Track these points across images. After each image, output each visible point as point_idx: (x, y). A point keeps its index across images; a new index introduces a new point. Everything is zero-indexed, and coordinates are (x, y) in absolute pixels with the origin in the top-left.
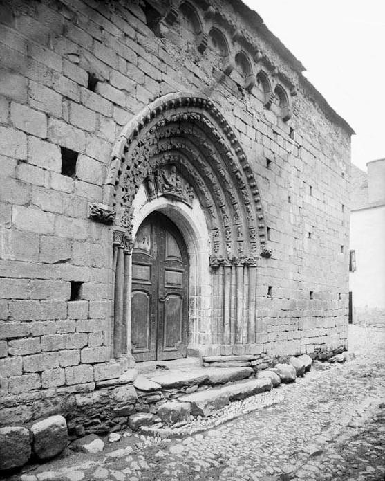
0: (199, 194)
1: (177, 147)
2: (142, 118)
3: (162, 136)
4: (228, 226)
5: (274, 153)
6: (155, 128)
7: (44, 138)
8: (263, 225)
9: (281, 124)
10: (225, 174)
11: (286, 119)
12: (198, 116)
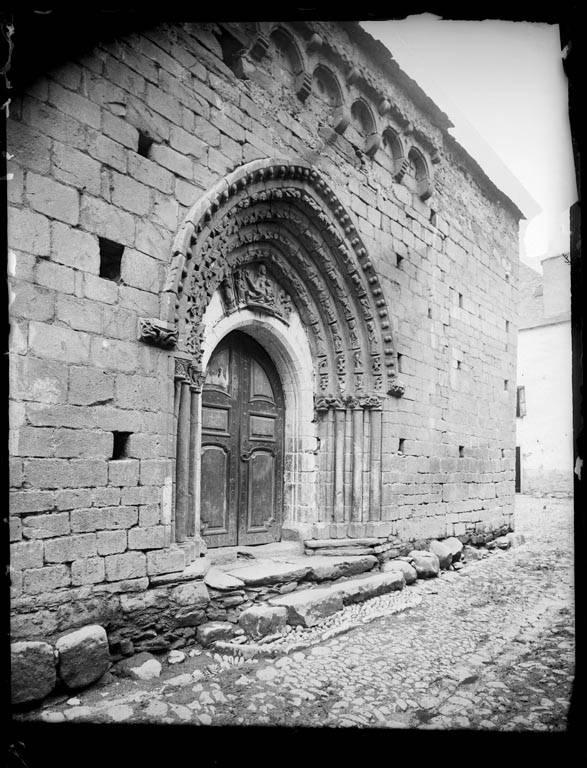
0: (299, 305)
1: (267, 237)
2: (217, 195)
3: (245, 222)
5: (407, 246)
6: (235, 210)
7: (75, 224)
8: (391, 350)
9: (418, 205)
10: (337, 276)
11: (424, 197)
12: (298, 193)
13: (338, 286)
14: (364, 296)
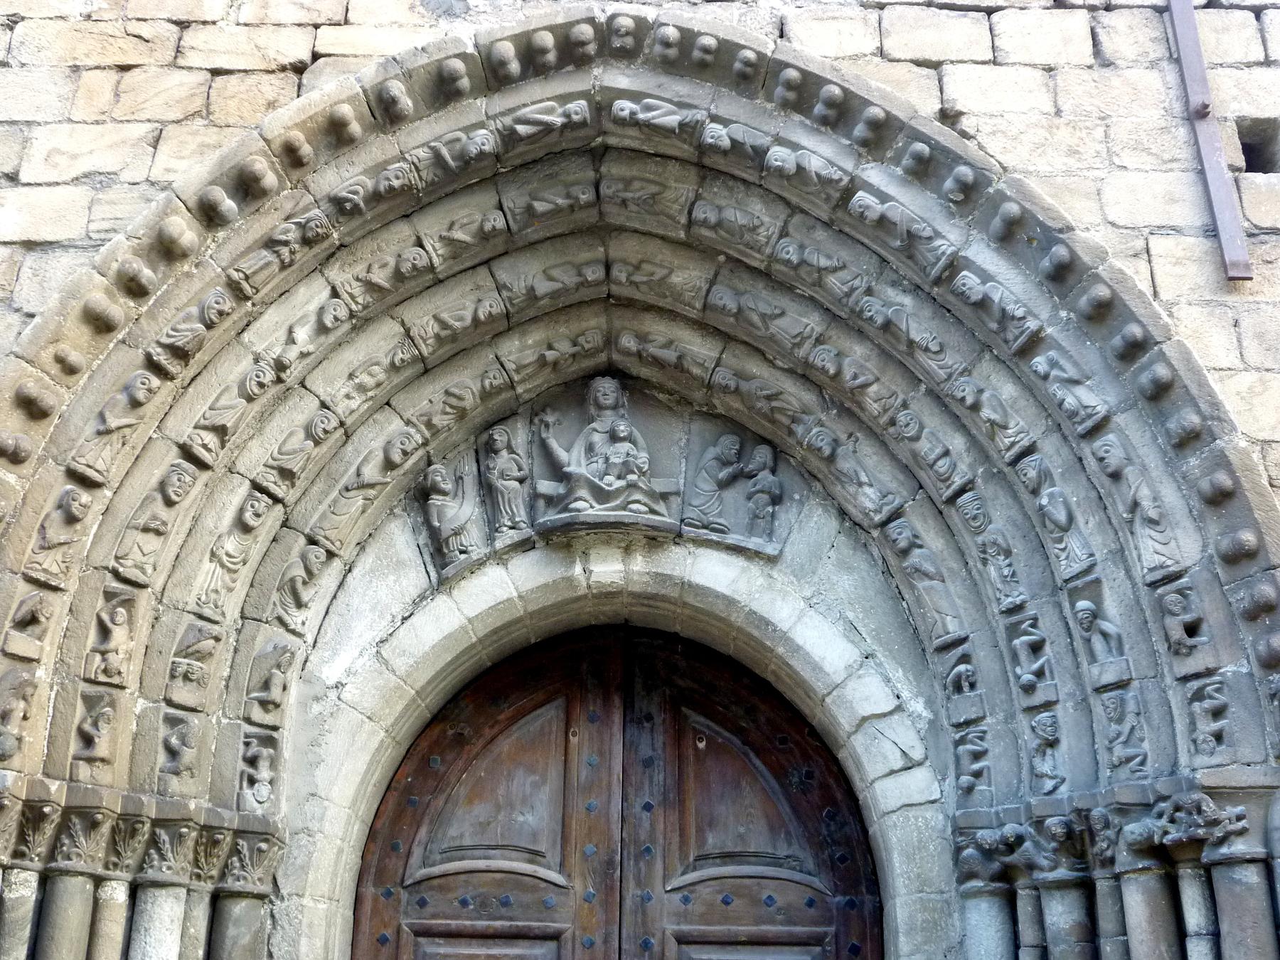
0: (819, 476)
4: (1018, 608)
13: (911, 343)
14: (1034, 342)
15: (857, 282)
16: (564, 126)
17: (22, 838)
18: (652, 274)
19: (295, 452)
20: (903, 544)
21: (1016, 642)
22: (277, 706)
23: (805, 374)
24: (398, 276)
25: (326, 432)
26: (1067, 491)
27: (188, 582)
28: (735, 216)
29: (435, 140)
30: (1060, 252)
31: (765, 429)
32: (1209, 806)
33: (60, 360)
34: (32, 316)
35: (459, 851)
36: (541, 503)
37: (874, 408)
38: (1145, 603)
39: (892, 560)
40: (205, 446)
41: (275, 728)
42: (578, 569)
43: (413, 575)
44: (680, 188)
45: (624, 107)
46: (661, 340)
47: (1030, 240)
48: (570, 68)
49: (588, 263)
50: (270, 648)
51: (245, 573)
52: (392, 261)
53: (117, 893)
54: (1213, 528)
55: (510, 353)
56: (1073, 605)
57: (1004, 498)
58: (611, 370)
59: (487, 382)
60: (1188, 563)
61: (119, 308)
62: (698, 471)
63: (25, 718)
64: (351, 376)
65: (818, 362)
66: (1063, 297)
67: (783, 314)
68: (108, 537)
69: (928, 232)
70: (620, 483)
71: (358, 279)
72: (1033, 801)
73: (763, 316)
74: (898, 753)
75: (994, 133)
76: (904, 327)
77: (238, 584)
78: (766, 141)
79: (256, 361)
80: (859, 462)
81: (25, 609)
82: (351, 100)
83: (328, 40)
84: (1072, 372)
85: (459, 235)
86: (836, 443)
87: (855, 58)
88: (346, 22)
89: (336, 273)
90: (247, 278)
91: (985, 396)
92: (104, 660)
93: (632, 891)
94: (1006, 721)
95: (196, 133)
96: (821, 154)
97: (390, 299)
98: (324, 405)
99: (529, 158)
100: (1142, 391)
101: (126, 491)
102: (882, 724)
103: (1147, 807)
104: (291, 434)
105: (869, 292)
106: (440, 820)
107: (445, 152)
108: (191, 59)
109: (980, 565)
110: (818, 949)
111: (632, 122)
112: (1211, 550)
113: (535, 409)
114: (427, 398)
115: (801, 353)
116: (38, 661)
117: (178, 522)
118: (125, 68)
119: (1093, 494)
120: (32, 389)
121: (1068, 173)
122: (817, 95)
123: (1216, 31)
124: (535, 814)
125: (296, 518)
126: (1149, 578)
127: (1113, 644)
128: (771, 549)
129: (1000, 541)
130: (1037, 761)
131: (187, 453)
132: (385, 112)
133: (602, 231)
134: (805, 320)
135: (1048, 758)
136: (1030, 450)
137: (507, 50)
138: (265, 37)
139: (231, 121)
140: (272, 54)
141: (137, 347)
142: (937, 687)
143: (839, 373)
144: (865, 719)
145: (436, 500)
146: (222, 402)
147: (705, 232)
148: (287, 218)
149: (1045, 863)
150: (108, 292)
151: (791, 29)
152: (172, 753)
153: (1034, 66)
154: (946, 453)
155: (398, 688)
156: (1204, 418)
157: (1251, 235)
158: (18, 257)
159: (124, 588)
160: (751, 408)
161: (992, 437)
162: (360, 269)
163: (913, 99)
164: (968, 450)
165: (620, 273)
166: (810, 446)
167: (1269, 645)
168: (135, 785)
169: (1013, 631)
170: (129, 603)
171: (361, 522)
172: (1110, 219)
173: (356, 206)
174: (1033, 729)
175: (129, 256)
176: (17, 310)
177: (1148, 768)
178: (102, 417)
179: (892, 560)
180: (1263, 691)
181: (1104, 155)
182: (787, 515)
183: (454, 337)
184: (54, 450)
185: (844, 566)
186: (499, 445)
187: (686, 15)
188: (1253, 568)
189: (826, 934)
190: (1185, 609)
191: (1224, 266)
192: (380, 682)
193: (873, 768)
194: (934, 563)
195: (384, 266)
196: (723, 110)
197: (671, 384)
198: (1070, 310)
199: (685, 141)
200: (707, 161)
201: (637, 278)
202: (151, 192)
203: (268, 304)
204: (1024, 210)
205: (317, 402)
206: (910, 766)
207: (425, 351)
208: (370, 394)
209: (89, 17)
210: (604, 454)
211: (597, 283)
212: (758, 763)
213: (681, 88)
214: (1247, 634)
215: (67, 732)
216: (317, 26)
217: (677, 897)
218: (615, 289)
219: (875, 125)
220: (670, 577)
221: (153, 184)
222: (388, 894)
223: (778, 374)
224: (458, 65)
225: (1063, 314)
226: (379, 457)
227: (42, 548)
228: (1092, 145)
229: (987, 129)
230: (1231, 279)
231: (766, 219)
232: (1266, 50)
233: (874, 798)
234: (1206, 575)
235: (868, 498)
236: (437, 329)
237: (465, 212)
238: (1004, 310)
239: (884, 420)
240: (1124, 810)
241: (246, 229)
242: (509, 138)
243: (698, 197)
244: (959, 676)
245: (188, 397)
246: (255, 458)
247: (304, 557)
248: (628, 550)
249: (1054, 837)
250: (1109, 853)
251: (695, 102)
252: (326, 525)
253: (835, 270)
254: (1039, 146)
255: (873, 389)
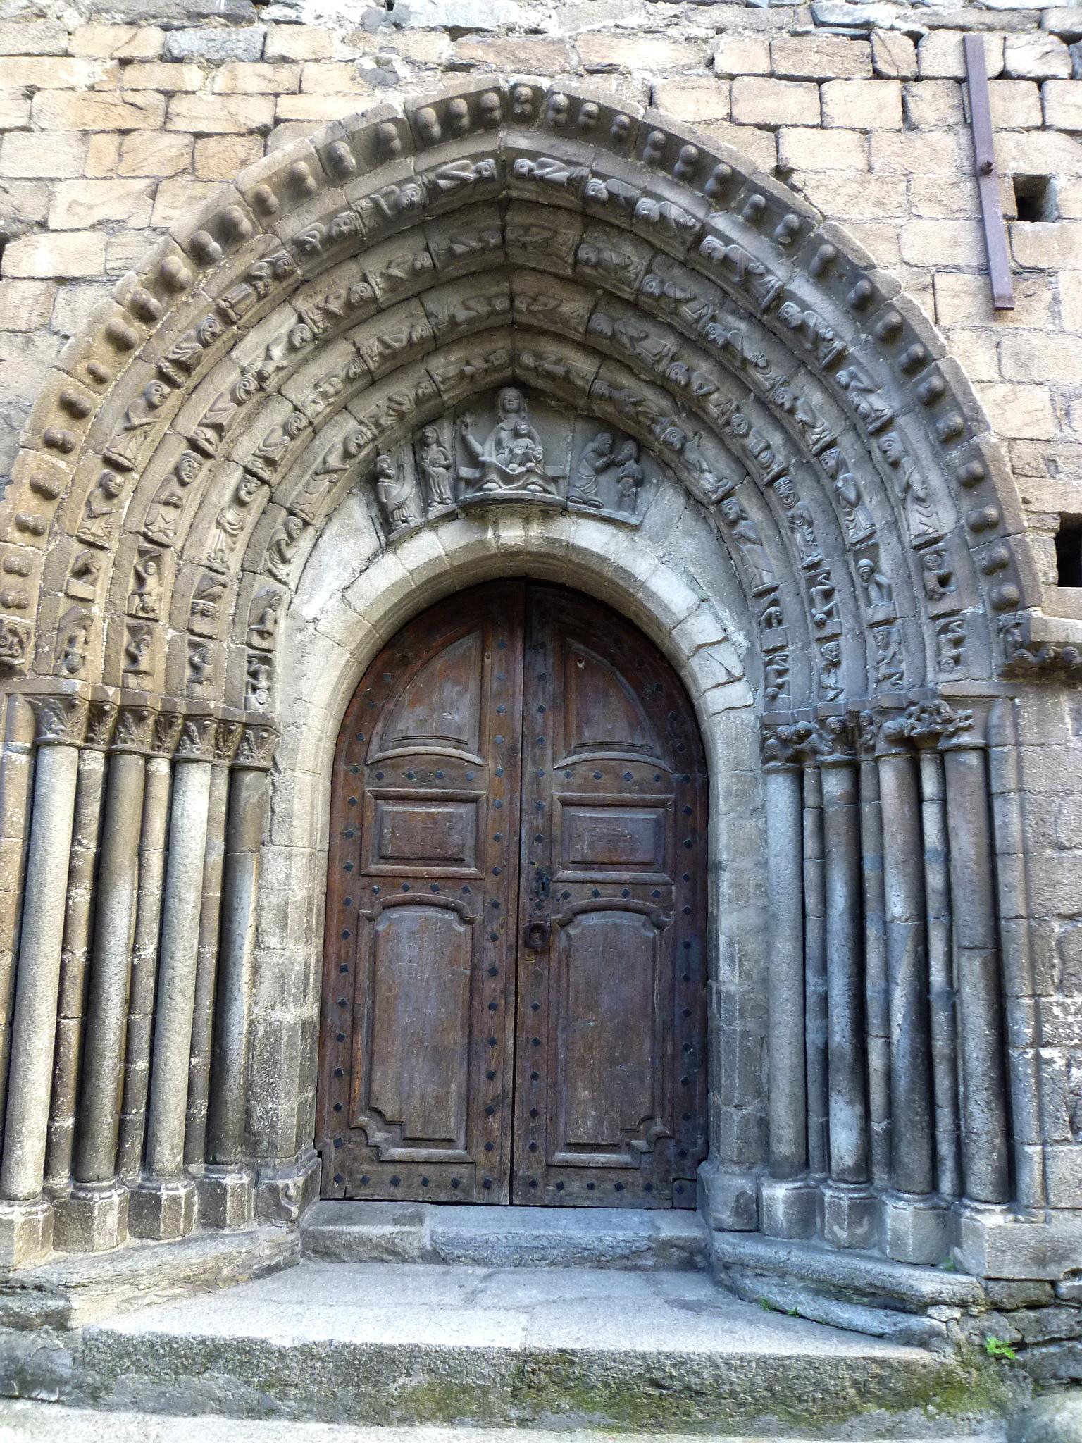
4: (815, 565)
13: (744, 360)
14: (840, 359)
15: (704, 311)
16: (477, 181)
17: (90, 728)
18: (546, 305)
19: (275, 445)
20: (732, 517)
21: (813, 590)
22: (271, 635)
23: (663, 385)
24: (349, 305)
25: (299, 429)
26: (858, 476)
27: (200, 544)
28: (611, 257)
29: (375, 192)
30: (864, 285)
31: (631, 428)
32: (946, 709)
33: (92, 372)
34: (67, 337)
35: (405, 740)
36: (462, 485)
37: (715, 411)
38: (910, 562)
39: (724, 529)
40: (207, 440)
41: (270, 651)
42: (490, 534)
43: (367, 539)
44: (569, 234)
45: (524, 164)
46: (553, 357)
47: (841, 276)
48: (481, 131)
49: (497, 296)
50: (263, 593)
51: (243, 537)
52: (344, 293)
53: (161, 767)
54: (966, 505)
55: (438, 368)
56: (856, 563)
57: (809, 482)
58: (515, 382)
59: (420, 391)
60: (945, 532)
61: (134, 330)
62: (580, 460)
63: (86, 642)
64: (316, 386)
65: (673, 376)
66: (863, 322)
67: (647, 337)
68: (138, 509)
69: (761, 270)
70: (521, 470)
71: (318, 308)
72: (819, 705)
73: (631, 339)
74: (724, 671)
75: (817, 187)
76: (739, 347)
77: (238, 546)
78: (637, 193)
79: (243, 372)
80: (702, 454)
81: (80, 563)
82: (306, 158)
83: (287, 106)
84: (866, 383)
85: (396, 272)
86: (685, 439)
87: (709, 122)
88: (301, 92)
89: (301, 303)
90: (232, 306)
91: (800, 402)
92: (142, 600)
93: (530, 769)
94: (803, 648)
95: (185, 187)
96: (678, 204)
97: (344, 325)
98: (296, 409)
99: (448, 208)
100: (920, 398)
101: (149, 474)
102: (712, 650)
103: (900, 710)
104: (272, 431)
105: (713, 319)
106: (391, 718)
107: (382, 202)
108: (179, 124)
109: (789, 533)
110: (662, 810)
111: (531, 177)
112: (963, 522)
113: (456, 413)
114: (375, 403)
115: (660, 368)
116: (92, 601)
117: (191, 498)
118: (124, 132)
119: (877, 479)
120: (72, 394)
121: (875, 220)
122: (677, 153)
123: (1005, 99)
124: (460, 716)
125: (279, 495)
126: (915, 543)
127: (885, 592)
128: (634, 520)
129: (805, 514)
130: (824, 677)
131: (193, 445)
132: (333, 169)
133: (507, 269)
134: (664, 342)
135: (832, 675)
136: (831, 444)
137: (430, 115)
138: (234, 104)
139: (213, 177)
140: (242, 120)
141: (150, 362)
142: (754, 624)
143: (688, 384)
144: (700, 646)
145: (384, 482)
146: (219, 406)
147: (588, 270)
148: (261, 258)
149: (825, 749)
150: (125, 318)
151: (660, 97)
152: (196, 668)
153: (853, 129)
154: (768, 447)
155: (358, 622)
156: (966, 420)
157: (1016, 273)
158: (53, 290)
159: (153, 549)
160: (621, 412)
161: (803, 434)
162: (319, 300)
163: (754, 157)
164: (785, 445)
165: (521, 304)
166: (665, 441)
167: (1000, 593)
168: (170, 691)
169: (812, 582)
170: (157, 559)
171: (328, 500)
172: (906, 258)
173: (314, 247)
174: (822, 653)
175: (139, 289)
176: (56, 333)
177: (904, 683)
178: (127, 417)
179: (724, 529)
180: (993, 627)
181: (904, 205)
182: (647, 495)
183: (394, 355)
184: (93, 442)
185: (689, 534)
186: (430, 440)
187: (574, 85)
188: (993, 535)
189: (668, 800)
190: (940, 566)
191: (992, 298)
192: (346, 618)
193: (705, 682)
194: (755, 531)
195: (338, 297)
196: (602, 167)
197: (560, 393)
198: (869, 334)
199: (571, 193)
200: (590, 211)
201: (535, 308)
202: (153, 236)
203: (249, 328)
204: (837, 251)
205: (291, 406)
206: (732, 680)
207: (372, 366)
208: (331, 400)
209: (92, 88)
210: (510, 448)
211: (503, 312)
212: (621, 678)
213: (569, 148)
214: (984, 586)
215: (118, 653)
216: (277, 95)
217: (562, 773)
218: (517, 317)
219: (724, 180)
220: (558, 540)
221: (154, 229)
222: (356, 770)
223: (642, 385)
224: (391, 128)
225: (863, 336)
226: (340, 448)
227: (90, 517)
228: (895, 199)
229: (814, 183)
230: (997, 308)
231: (635, 259)
232: (1043, 116)
233: (705, 704)
234: (958, 541)
235: (708, 482)
236: (381, 348)
237: (400, 253)
238: (817, 334)
239: (721, 422)
240: (884, 712)
241: (231, 266)
242: (432, 190)
243: (582, 241)
244: (770, 615)
245: (192, 402)
246: (246, 449)
247: (286, 525)
248: (527, 521)
249: (832, 731)
250: (871, 742)
251: (581, 160)
252: (302, 501)
253: (688, 301)
254: (852, 198)
255: (715, 396)
